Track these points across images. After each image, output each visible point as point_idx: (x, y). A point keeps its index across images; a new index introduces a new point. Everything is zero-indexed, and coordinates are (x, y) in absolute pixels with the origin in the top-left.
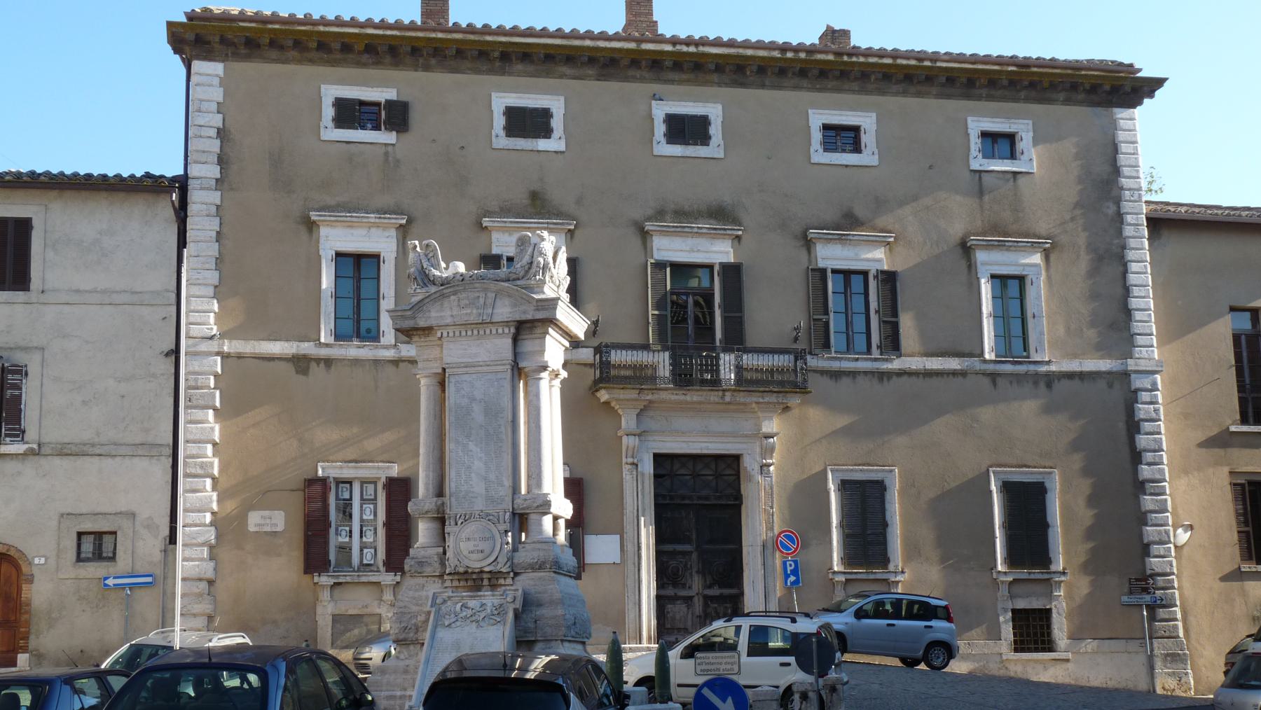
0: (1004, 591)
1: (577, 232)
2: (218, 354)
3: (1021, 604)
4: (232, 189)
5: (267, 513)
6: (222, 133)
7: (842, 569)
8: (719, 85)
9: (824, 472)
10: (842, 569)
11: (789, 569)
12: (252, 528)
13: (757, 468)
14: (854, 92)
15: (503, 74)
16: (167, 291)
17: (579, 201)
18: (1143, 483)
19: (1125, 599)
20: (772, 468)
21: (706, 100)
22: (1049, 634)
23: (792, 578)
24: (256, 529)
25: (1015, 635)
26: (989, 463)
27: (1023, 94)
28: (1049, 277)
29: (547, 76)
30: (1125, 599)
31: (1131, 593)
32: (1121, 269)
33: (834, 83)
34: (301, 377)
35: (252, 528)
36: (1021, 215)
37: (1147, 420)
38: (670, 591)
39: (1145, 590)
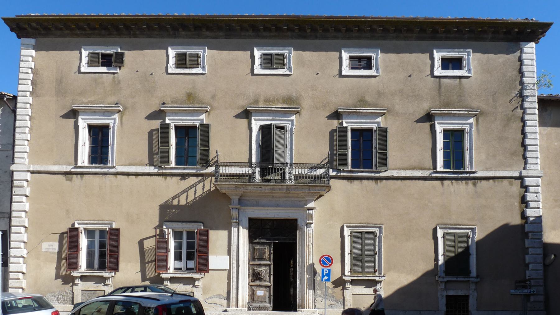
0: (442, 286)
1: (211, 112)
2: (28, 171)
3: (451, 293)
4: (37, 96)
5: (51, 243)
6: (35, 71)
7: (349, 274)
8: (292, 38)
9: (436, 227)
10: (349, 274)
11: (325, 273)
12: (44, 250)
13: (304, 224)
14: (368, 38)
15: (175, 38)
16: (9, 144)
17: (213, 97)
18: (527, 233)
19: (512, 291)
20: (312, 225)
21: (284, 46)
22: (467, 308)
23: (326, 278)
24: (46, 251)
25: (447, 308)
26: (438, 223)
27: (466, 36)
28: (478, 130)
29: (198, 38)
30: (512, 291)
31: (516, 288)
32: (521, 124)
33: (356, 34)
34: (68, 182)
35: (44, 250)
36: (463, 98)
37: (531, 201)
38: (257, 283)
39: (525, 287)
